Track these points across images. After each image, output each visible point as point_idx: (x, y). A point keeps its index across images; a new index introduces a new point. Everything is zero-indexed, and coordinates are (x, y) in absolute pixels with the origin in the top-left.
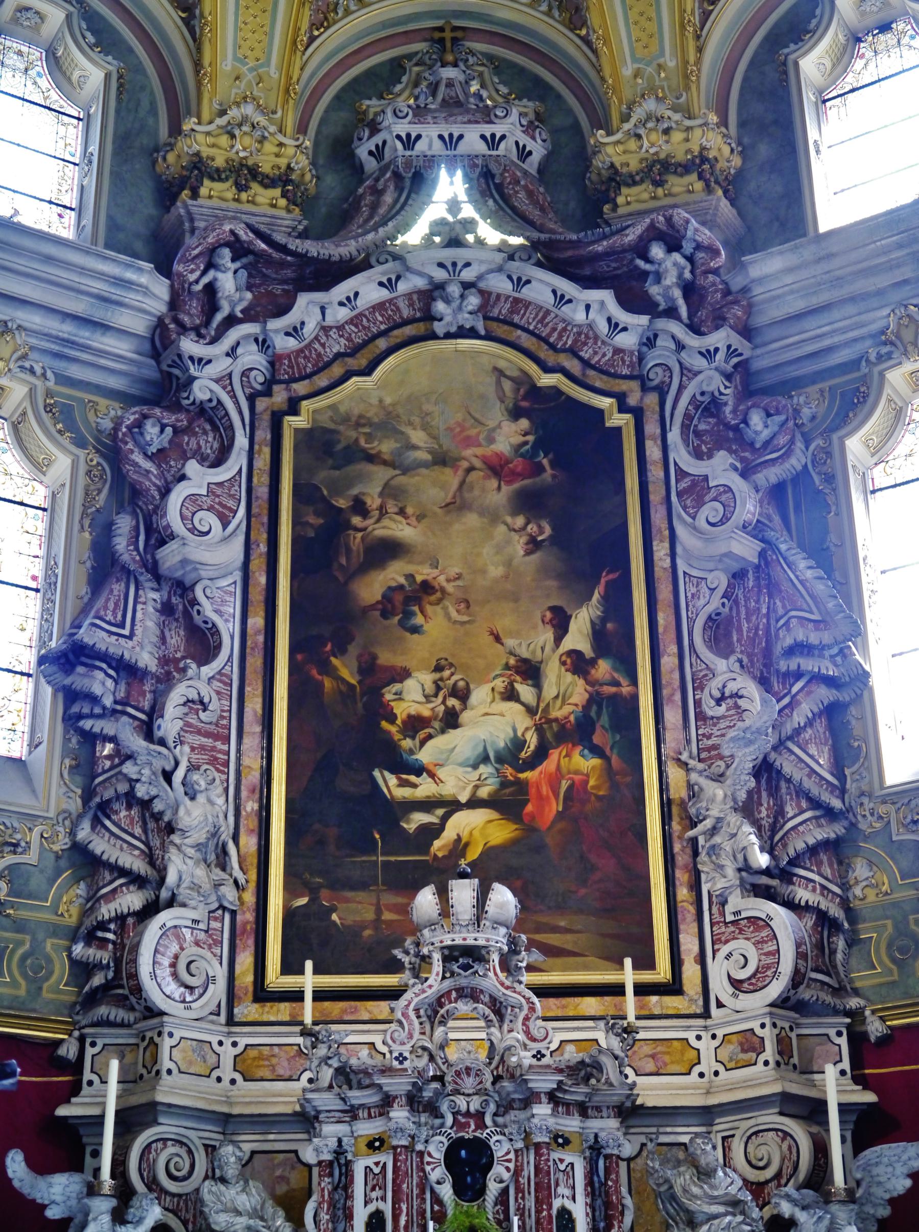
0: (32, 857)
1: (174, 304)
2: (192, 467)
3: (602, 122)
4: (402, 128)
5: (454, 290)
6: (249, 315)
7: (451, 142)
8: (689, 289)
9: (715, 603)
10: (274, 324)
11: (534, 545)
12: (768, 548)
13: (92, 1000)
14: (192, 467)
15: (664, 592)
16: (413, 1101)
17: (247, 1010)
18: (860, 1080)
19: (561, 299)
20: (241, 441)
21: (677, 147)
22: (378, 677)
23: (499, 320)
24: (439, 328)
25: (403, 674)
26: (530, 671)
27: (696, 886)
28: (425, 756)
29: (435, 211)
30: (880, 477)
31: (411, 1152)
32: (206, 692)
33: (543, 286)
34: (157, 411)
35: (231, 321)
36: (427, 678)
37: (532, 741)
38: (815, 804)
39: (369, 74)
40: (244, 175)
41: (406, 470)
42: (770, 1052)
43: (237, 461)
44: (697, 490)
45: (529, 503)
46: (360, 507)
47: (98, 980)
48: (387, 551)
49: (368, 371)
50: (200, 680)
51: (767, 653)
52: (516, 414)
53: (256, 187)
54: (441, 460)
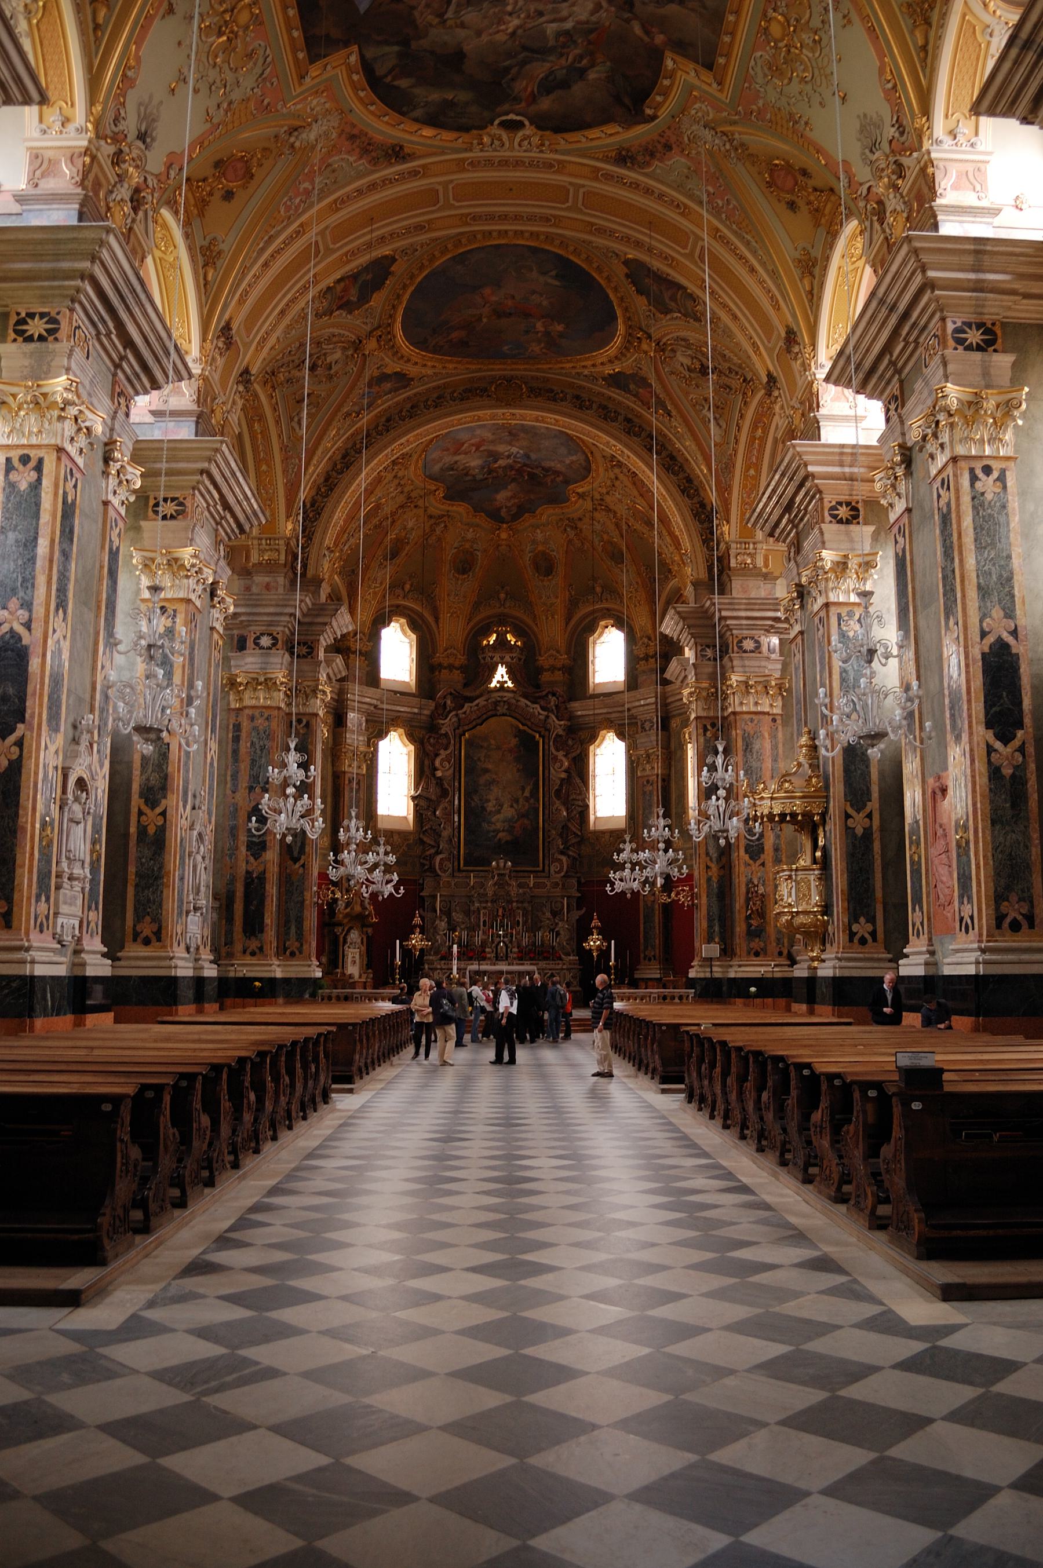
2: (442, 752)
6: (454, 709)
7: (502, 658)
8: (557, 706)
12: (569, 777)
14: (442, 752)
16: (492, 901)
23: (512, 710)
25: (488, 801)
26: (517, 801)
28: (493, 820)
29: (497, 677)
30: (598, 751)
33: (523, 701)
35: (450, 712)
40: (451, 667)
43: (451, 748)
44: (555, 758)
48: (487, 771)
54: (498, 748)
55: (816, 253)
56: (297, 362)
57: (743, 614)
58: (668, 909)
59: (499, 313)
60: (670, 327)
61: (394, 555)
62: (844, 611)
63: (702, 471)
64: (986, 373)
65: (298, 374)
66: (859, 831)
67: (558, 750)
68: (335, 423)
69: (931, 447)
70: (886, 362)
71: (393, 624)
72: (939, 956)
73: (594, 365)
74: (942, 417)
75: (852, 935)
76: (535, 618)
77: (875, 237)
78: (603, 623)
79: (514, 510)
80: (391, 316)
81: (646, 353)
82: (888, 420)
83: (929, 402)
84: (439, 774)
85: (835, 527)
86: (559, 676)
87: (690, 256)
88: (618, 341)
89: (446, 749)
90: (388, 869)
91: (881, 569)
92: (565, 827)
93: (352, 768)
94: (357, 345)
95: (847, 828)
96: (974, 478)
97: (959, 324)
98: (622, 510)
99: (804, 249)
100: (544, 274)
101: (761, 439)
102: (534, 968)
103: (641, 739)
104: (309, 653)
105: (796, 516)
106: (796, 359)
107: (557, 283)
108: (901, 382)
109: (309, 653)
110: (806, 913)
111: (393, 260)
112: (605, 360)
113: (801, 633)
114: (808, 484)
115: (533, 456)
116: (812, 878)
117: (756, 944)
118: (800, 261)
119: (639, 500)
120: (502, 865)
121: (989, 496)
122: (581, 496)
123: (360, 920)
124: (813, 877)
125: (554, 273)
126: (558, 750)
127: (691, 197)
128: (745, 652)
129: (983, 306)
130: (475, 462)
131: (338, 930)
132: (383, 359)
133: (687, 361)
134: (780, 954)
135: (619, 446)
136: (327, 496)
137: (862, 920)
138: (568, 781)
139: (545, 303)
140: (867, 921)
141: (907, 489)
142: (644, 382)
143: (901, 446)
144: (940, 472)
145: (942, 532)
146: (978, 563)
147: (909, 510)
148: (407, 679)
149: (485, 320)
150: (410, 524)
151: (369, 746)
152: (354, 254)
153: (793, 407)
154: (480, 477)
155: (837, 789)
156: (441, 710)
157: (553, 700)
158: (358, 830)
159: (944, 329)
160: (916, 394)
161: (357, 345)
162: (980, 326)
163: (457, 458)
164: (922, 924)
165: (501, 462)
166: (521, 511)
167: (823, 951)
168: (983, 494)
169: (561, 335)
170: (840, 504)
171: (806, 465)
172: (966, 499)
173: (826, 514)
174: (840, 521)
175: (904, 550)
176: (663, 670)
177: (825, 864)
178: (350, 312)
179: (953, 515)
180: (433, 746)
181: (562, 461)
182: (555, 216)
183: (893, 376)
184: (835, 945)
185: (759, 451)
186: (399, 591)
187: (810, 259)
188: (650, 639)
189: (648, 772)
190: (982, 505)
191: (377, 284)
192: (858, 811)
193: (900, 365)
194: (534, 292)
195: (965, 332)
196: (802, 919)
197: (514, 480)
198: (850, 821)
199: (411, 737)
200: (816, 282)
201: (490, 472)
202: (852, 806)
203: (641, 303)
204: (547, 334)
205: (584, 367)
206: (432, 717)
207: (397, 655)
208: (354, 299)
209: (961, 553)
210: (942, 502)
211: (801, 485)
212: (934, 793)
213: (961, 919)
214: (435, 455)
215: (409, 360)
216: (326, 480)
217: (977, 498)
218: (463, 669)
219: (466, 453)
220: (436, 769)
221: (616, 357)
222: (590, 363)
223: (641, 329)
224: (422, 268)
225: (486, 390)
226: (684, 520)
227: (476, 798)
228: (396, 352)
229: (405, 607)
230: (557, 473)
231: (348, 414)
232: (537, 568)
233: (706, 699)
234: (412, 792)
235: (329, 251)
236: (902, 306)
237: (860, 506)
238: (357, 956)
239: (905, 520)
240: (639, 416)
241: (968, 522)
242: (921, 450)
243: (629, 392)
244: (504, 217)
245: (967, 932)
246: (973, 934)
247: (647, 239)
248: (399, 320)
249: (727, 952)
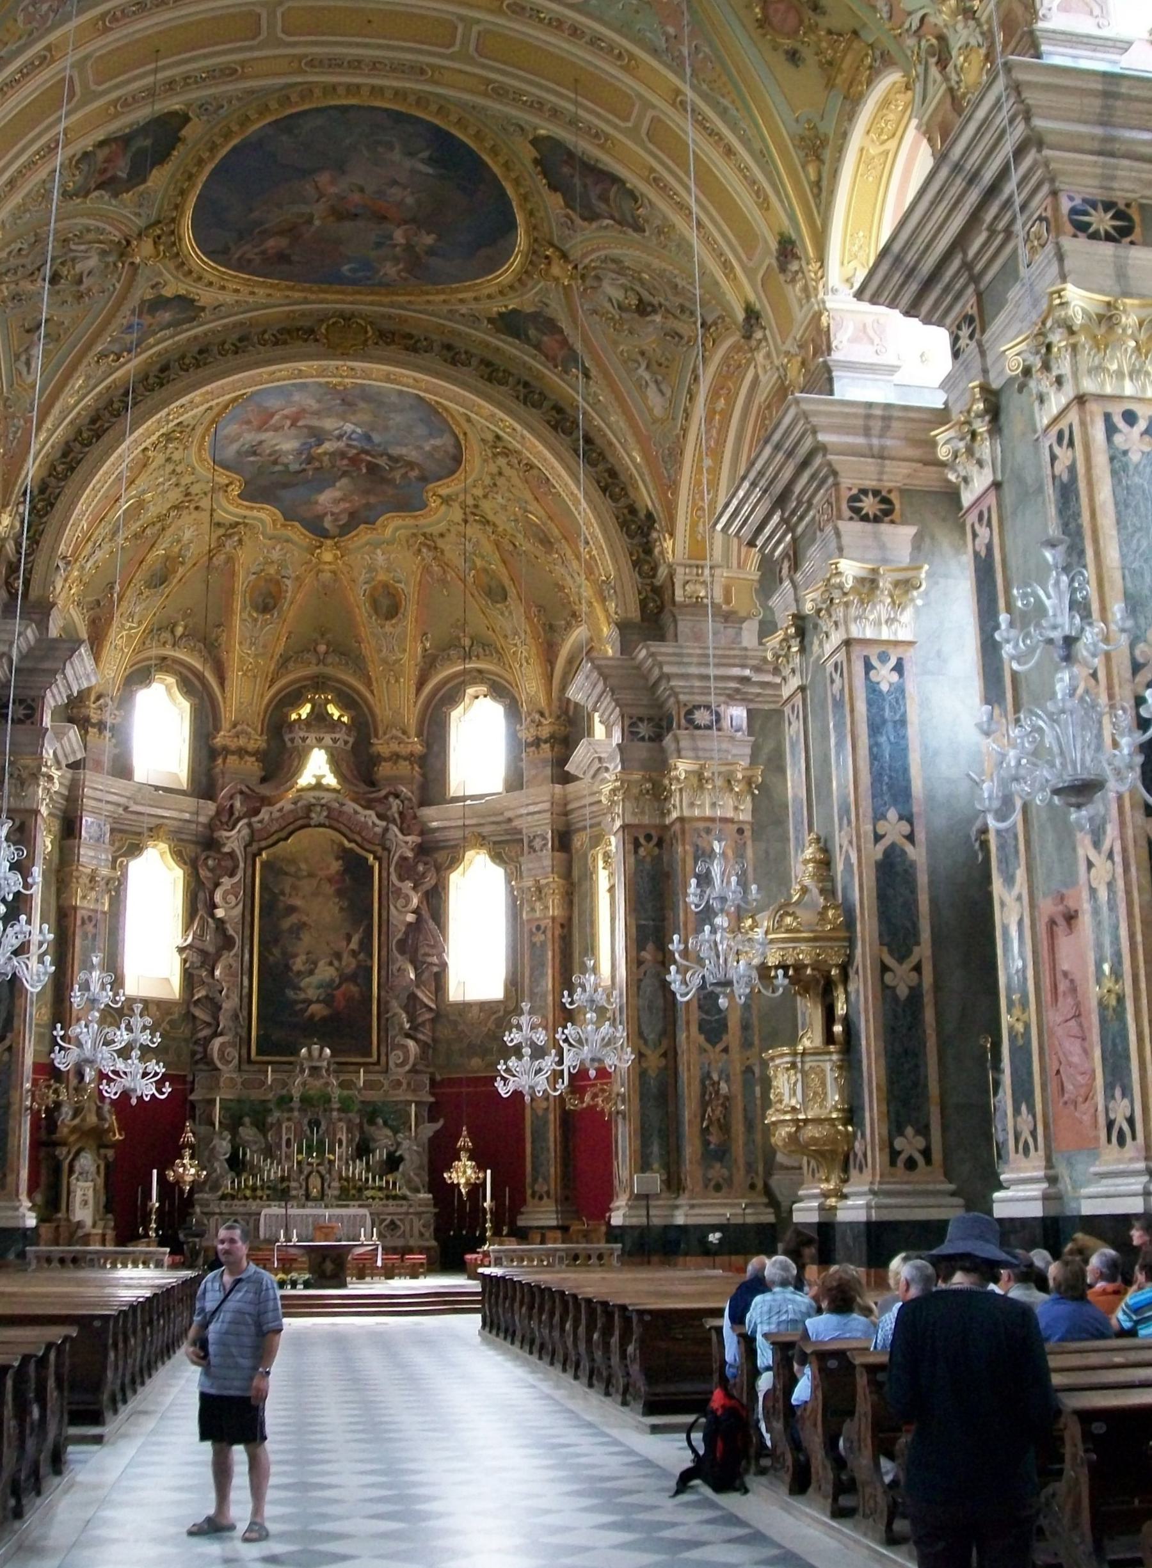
0: (176, 1016)
1: (218, 813)
3: (376, 736)
4: (302, 734)
5: (318, 809)
7: (320, 740)
8: (401, 814)
9: (400, 936)
10: (254, 819)
11: (341, 909)
13: (196, 1063)
15: (384, 929)
17: (245, 1067)
18: (432, 1094)
19: (356, 812)
20: (242, 865)
21: (404, 750)
22: (288, 956)
23: (334, 819)
24: (313, 823)
25: (295, 956)
26: (338, 956)
27: (387, 1030)
28: (302, 984)
31: (300, 1123)
32: (231, 961)
33: (351, 806)
34: (213, 854)
36: (304, 957)
37: (337, 980)
38: (426, 1006)
39: (289, 694)
40: (241, 752)
41: (299, 878)
42: (405, 1086)
43: (240, 874)
45: (340, 893)
46: (283, 893)
47: (198, 1056)
48: (292, 909)
49: (286, 839)
50: (228, 958)
51: (416, 950)
52: (337, 858)
53: (247, 758)
54: (311, 875)
55: (828, 128)
56: (30, 268)
57: (694, 670)
58: (569, 1121)
59: (340, 213)
60: (593, 241)
61: (159, 579)
62: (873, 653)
63: (633, 460)
64: (1121, 274)
65: (30, 287)
66: (903, 992)
67: (401, 879)
68: (82, 368)
69: (1041, 383)
70: (956, 263)
71: (155, 685)
72: (1066, 1185)
73: (476, 299)
74: (1058, 339)
75: (894, 1155)
76: (369, 684)
77: (931, 90)
78: (471, 691)
79: (344, 519)
80: (176, 207)
81: (556, 279)
82: (956, 354)
83: (1034, 317)
84: (220, 913)
85: (858, 526)
86: (404, 768)
87: (633, 133)
88: (516, 262)
89: (232, 875)
90: (146, 1052)
91: (926, 593)
92: (413, 997)
93: (85, 901)
94: (123, 249)
95: (885, 987)
96: (1111, 430)
97: (1078, 201)
98: (501, 521)
99: (809, 121)
100: (411, 154)
101: (722, 412)
102: (365, 1211)
103: (528, 863)
104: (28, 716)
105: (793, 513)
106: (793, 281)
107: (430, 171)
108: (979, 295)
109: (28, 716)
110: (817, 1121)
111: (186, 119)
112: (492, 290)
113: (802, 689)
114: (818, 461)
115: (376, 438)
116: (828, 1066)
117: (717, 1171)
118: (802, 139)
119: (533, 506)
120: (316, 1053)
121: (1135, 457)
122: (446, 500)
123: (97, 1137)
124: (829, 1066)
125: (425, 154)
126: (401, 879)
127: (640, 42)
128: (698, 727)
129: (1113, 178)
130: (288, 445)
131: (61, 1152)
132: (161, 274)
133: (617, 294)
134: (752, 1187)
135: (509, 421)
136: (66, 478)
137: (909, 1131)
138: (415, 928)
139: (410, 200)
141: (993, 451)
142: (551, 326)
143: (985, 389)
144: (1055, 420)
145: (1061, 512)
146: (1123, 556)
147: (997, 485)
148: (175, 769)
149: (317, 223)
150: (187, 535)
151: (114, 868)
152: (127, 103)
153: (787, 353)
154: (295, 467)
155: (867, 928)
156: (226, 817)
157: (395, 804)
158: (103, 987)
159: (1056, 209)
160: (1009, 307)
161: (123, 249)
162: (1108, 206)
163: (264, 436)
164: (1033, 1133)
165: (328, 446)
166: (354, 520)
167: (845, 1181)
168: (1125, 453)
169: (431, 252)
170: (864, 492)
171: (814, 432)
172: (1101, 459)
173: (844, 506)
174: (865, 518)
175: (989, 547)
176: (564, 760)
177: (849, 1045)
178: (116, 195)
179: (1082, 485)
180: (211, 870)
181: (417, 447)
182: (433, 67)
183: (965, 286)
184: (868, 1171)
185: (719, 433)
186: (166, 635)
187: (817, 137)
188: (542, 714)
189: (538, 914)
190: (1125, 468)
191: (160, 156)
192: (901, 960)
193: (978, 268)
194: (394, 183)
195: (1086, 213)
196: (811, 1132)
197: (345, 474)
198: (888, 977)
199: (178, 855)
200: (826, 170)
201: (310, 460)
202: (891, 952)
203: (555, 201)
204: (409, 247)
205: (462, 301)
206: (210, 827)
207: (159, 735)
208: (123, 175)
209: (1096, 541)
210: (1060, 467)
211: (805, 464)
212: (1052, 923)
213: (1110, 1124)
214: (232, 429)
215: (200, 278)
216: (65, 455)
217: (1117, 457)
218: (261, 756)
219: (276, 429)
220: (215, 906)
221: (511, 287)
222: (469, 295)
223: (552, 245)
224: (228, 135)
225: (311, 331)
226: (605, 531)
227: (276, 951)
228: (181, 265)
229: (176, 661)
230: (411, 465)
231: (103, 355)
232: (375, 604)
233: (637, 799)
234: (180, 942)
235: (90, 96)
236: (988, 175)
237: (894, 497)
238: (90, 1193)
239: (991, 499)
240: (540, 377)
241: (1105, 493)
242: (1021, 389)
243: (528, 340)
244: (356, 64)
245: (1121, 1142)
246: (1132, 1148)
247: (572, 108)
248: (189, 213)
249: (674, 1184)
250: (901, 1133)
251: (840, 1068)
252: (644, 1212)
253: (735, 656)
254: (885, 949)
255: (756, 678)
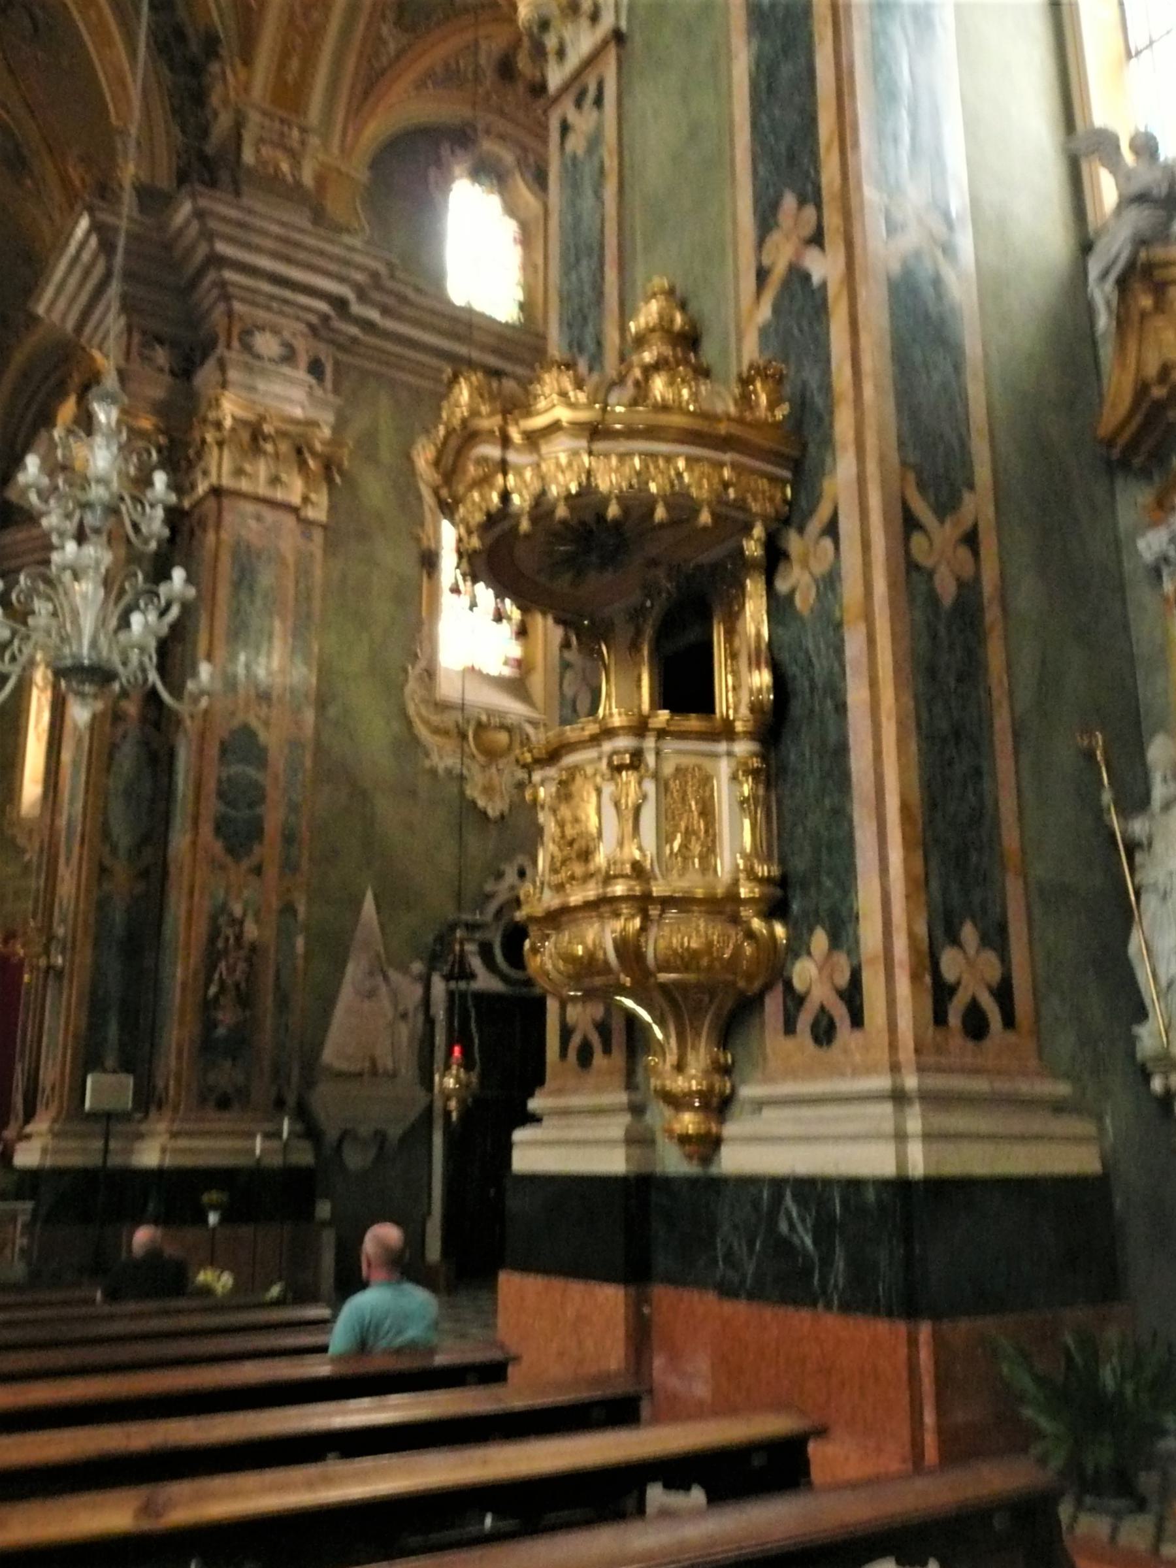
57: (265, 263)
116: (724, 768)
117: (225, 1075)
140: (985, 941)
202: (922, 486)
250: (954, 940)
251: (755, 773)
252: (99, 1144)
253: (331, 257)
254: (911, 477)
255: (356, 308)
